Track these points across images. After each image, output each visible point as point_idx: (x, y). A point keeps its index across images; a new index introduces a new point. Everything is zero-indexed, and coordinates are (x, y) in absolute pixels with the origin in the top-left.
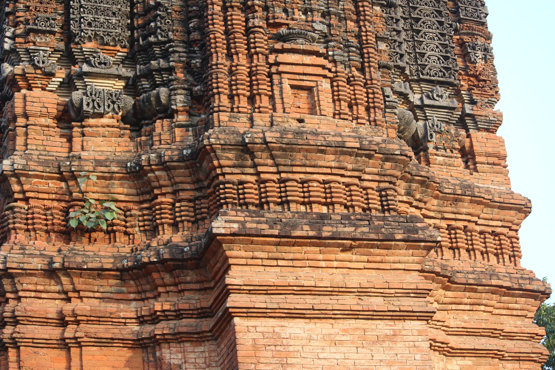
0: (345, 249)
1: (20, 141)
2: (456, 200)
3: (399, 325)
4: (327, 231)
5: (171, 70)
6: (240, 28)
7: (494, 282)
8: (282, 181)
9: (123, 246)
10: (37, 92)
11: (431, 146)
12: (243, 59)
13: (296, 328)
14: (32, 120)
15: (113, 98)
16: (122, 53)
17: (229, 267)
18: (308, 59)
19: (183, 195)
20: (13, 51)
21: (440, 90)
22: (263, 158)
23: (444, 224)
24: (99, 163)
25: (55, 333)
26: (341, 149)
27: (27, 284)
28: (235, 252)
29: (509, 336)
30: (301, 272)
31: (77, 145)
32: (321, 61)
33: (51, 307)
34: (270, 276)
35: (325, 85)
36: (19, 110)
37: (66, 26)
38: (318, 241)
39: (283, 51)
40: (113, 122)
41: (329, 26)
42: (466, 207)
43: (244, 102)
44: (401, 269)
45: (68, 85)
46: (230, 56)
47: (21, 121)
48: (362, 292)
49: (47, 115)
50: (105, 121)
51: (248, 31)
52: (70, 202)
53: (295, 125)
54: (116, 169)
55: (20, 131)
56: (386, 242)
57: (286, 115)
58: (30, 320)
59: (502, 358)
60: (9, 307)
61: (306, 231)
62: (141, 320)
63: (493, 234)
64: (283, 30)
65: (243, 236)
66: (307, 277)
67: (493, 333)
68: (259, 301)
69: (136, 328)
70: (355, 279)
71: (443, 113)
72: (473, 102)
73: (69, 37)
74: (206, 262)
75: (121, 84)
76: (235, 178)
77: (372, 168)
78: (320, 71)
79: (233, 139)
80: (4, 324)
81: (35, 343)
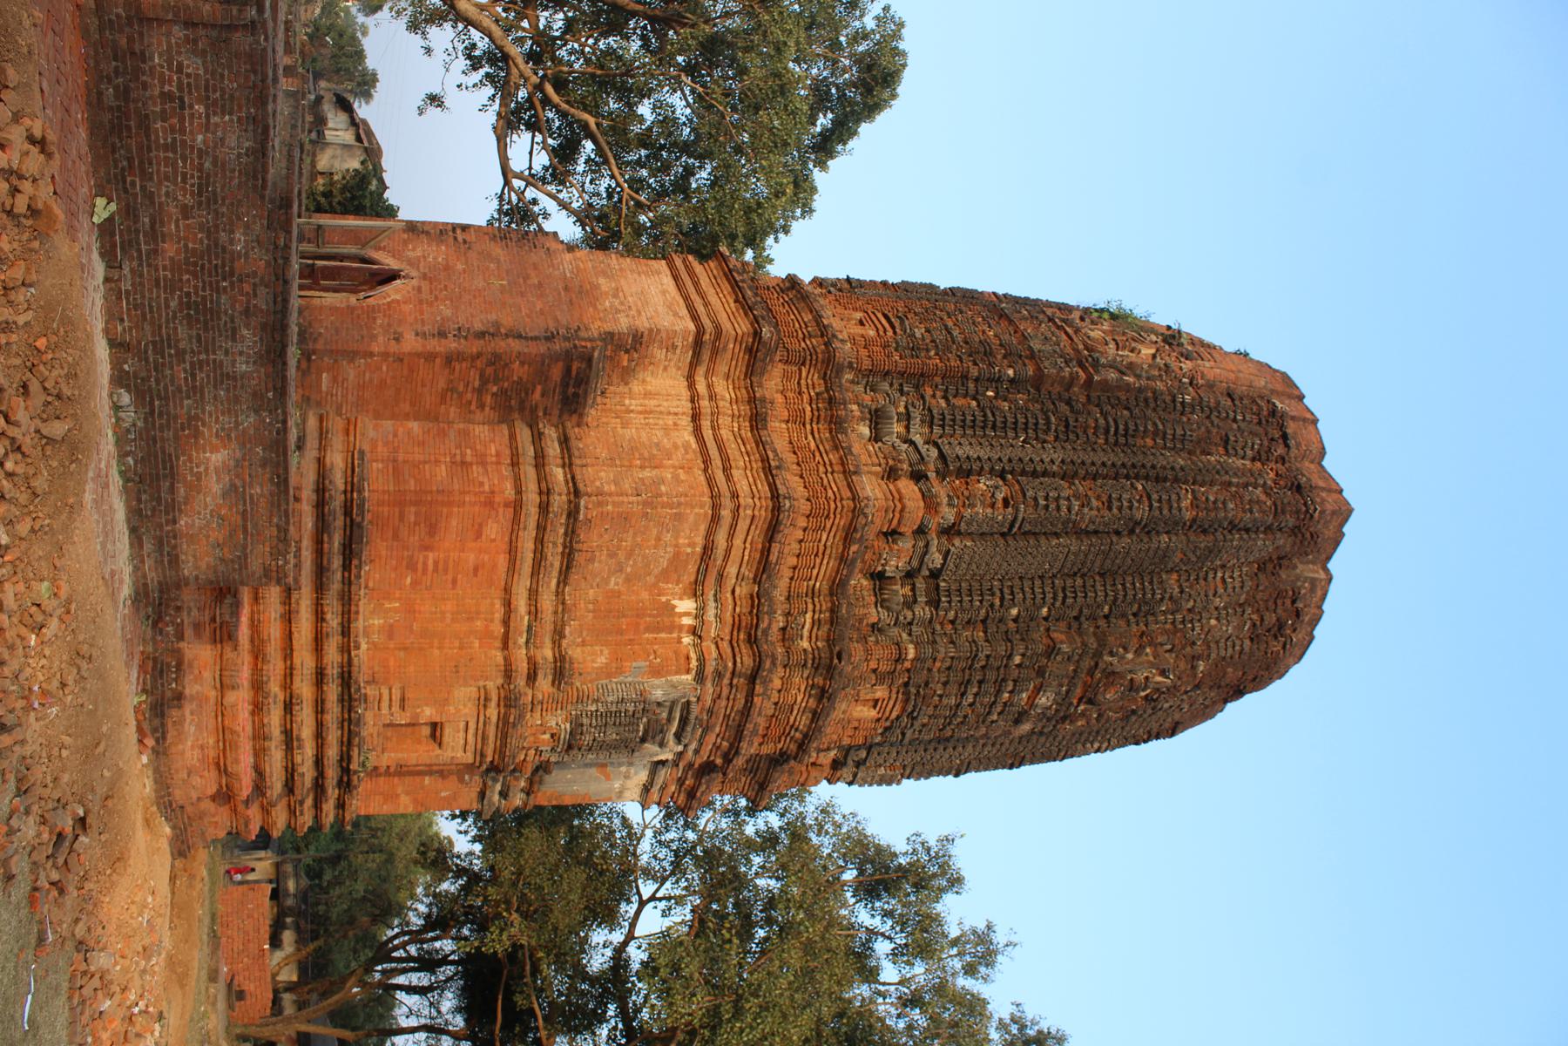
2: (836, 448)
26: (818, 318)
42: (834, 457)
59: (705, 470)
67: (725, 459)
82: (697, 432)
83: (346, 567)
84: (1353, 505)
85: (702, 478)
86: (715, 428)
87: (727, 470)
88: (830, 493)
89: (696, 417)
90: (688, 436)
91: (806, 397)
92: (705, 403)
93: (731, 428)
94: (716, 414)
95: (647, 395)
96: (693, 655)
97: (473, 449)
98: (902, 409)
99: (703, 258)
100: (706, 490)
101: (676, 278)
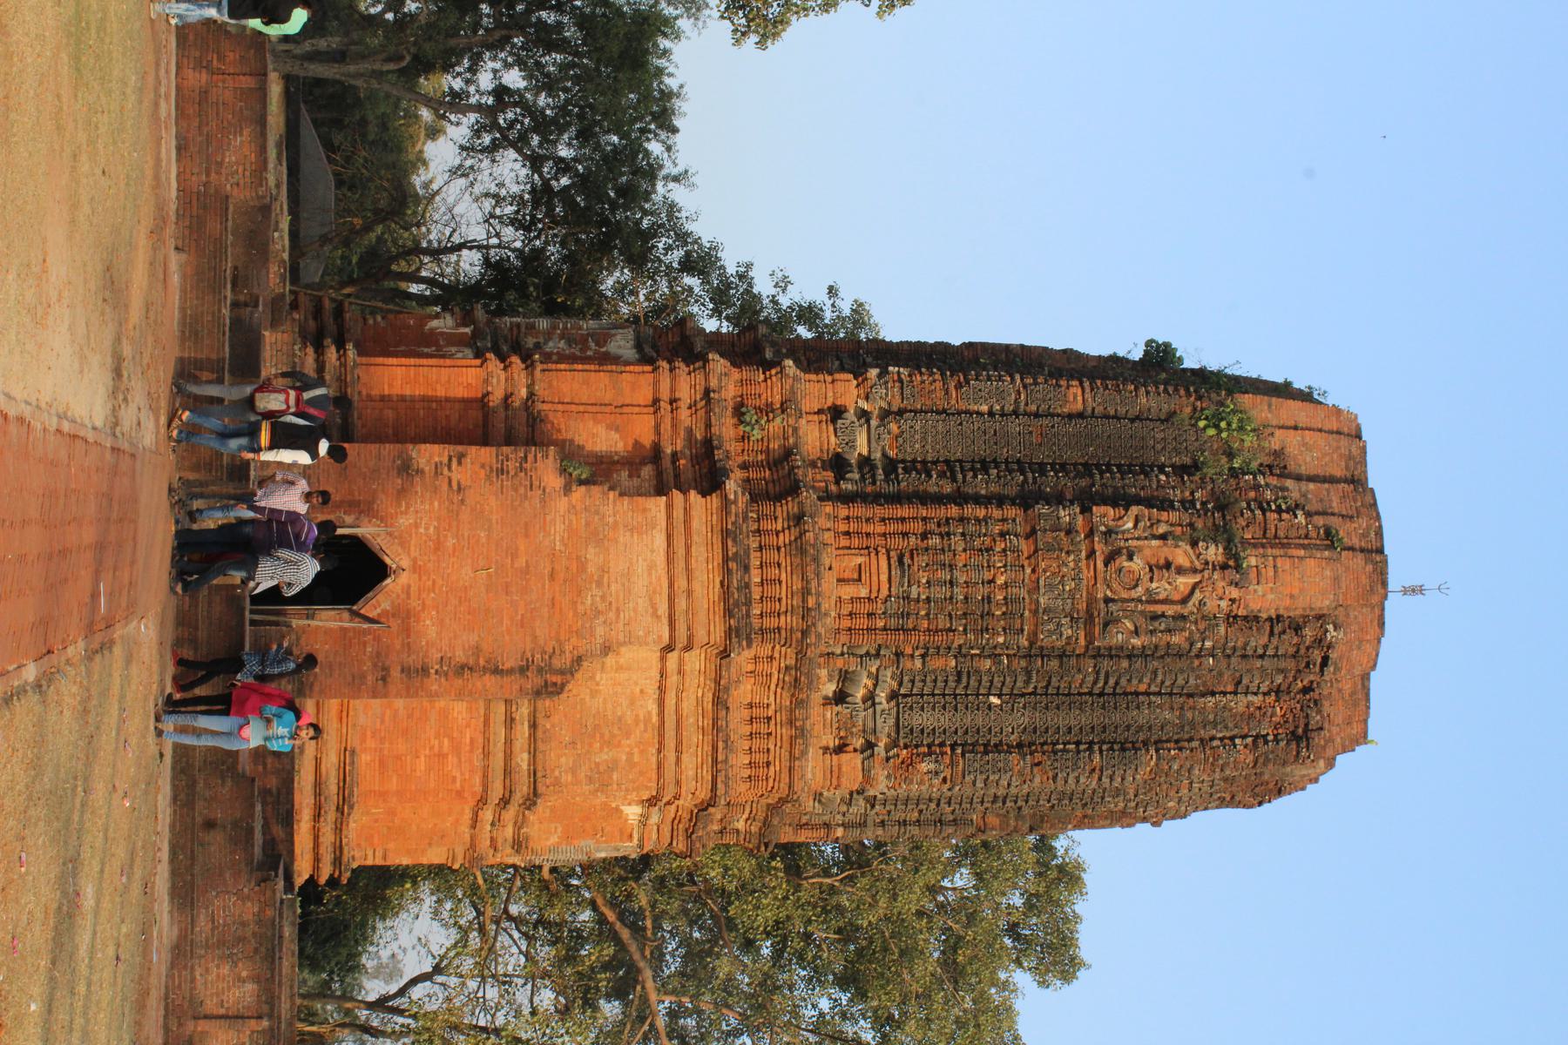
0: (722, 583)
1: (813, 377)
2: (791, 722)
3: (665, 621)
4: (733, 565)
5: (874, 483)
6: (907, 527)
7: (721, 745)
8: (779, 549)
9: (733, 447)
10: (855, 392)
11: (839, 708)
12: (880, 529)
13: (660, 540)
14: (830, 386)
15: (851, 444)
16: (891, 454)
17: (704, 496)
18: (884, 578)
19: (771, 486)
20: (888, 373)
21: (892, 721)
22: (795, 532)
23: (771, 713)
24: (795, 430)
25: (665, 395)
26: (805, 592)
27: (700, 377)
28: (715, 500)
29: (678, 761)
30: (703, 549)
31: (810, 417)
32: (884, 592)
33: (685, 393)
34: (698, 523)
35: (864, 593)
36: (837, 376)
37: (906, 411)
38: (726, 559)
39: (889, 558)
40: (832, 446)
41: (918, 601)
42: (786, 732)
43: (843, 527)
44: (710, 629)
45: (864, 415)
46: (883, 520)
47: (829, 379)
48: (689, 593)
49: (835, 398)
50: (833, 438)
51: (905, 535)
52: (767, 410)
53: (827, 562)
54: (791, 441)
55: (821, 377)
56: (728, 613)
57: (837, 562)
58: (673, 379)
59: (659, 751)
60: (682, 365)
61: (732, 550)
62: (675, 456)
63: (768, 764)
64: (907, 560)
65: (726, 504)
66: (699, 552)
68: (678, 513)
69: (669, 451)
70: (698, 588)
71: (870, 724)
72: (888, 759)
73: (901, 412)
74: (710, 480)
75: (865, 452)
76: (779, 513)
77: (793, 621)
78: (875, 588)
79: (807, 509)
80: (670, 362)
81: (656, 383)
82: (661, 703)
83: (340, 810)
84: (1411, 671)
85: (654, 759)
86: (679, 700)
87: (679, 751)
88: (772, 773)
89: (662, 690)
90: (653, 707)
91: (775, 664)
92: (673, 679)
93: (694, 693)
94: (680, 692)
95: (619, 668)
96: (636, 836)
97: (452, 739)
98: (874, 670)
99: (704, 494)
100: (654, 776)
101: (669, 537)
